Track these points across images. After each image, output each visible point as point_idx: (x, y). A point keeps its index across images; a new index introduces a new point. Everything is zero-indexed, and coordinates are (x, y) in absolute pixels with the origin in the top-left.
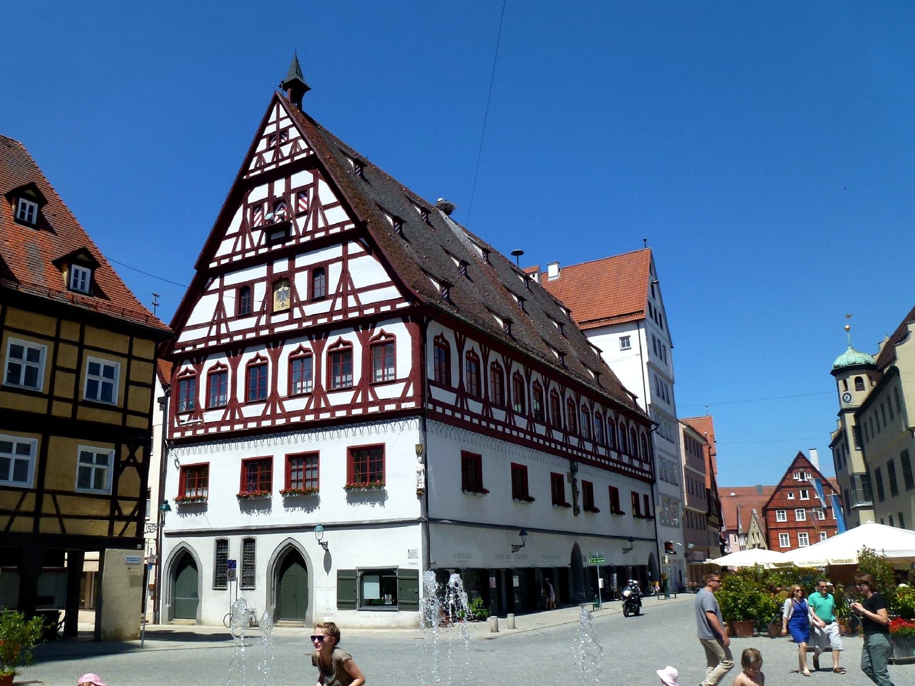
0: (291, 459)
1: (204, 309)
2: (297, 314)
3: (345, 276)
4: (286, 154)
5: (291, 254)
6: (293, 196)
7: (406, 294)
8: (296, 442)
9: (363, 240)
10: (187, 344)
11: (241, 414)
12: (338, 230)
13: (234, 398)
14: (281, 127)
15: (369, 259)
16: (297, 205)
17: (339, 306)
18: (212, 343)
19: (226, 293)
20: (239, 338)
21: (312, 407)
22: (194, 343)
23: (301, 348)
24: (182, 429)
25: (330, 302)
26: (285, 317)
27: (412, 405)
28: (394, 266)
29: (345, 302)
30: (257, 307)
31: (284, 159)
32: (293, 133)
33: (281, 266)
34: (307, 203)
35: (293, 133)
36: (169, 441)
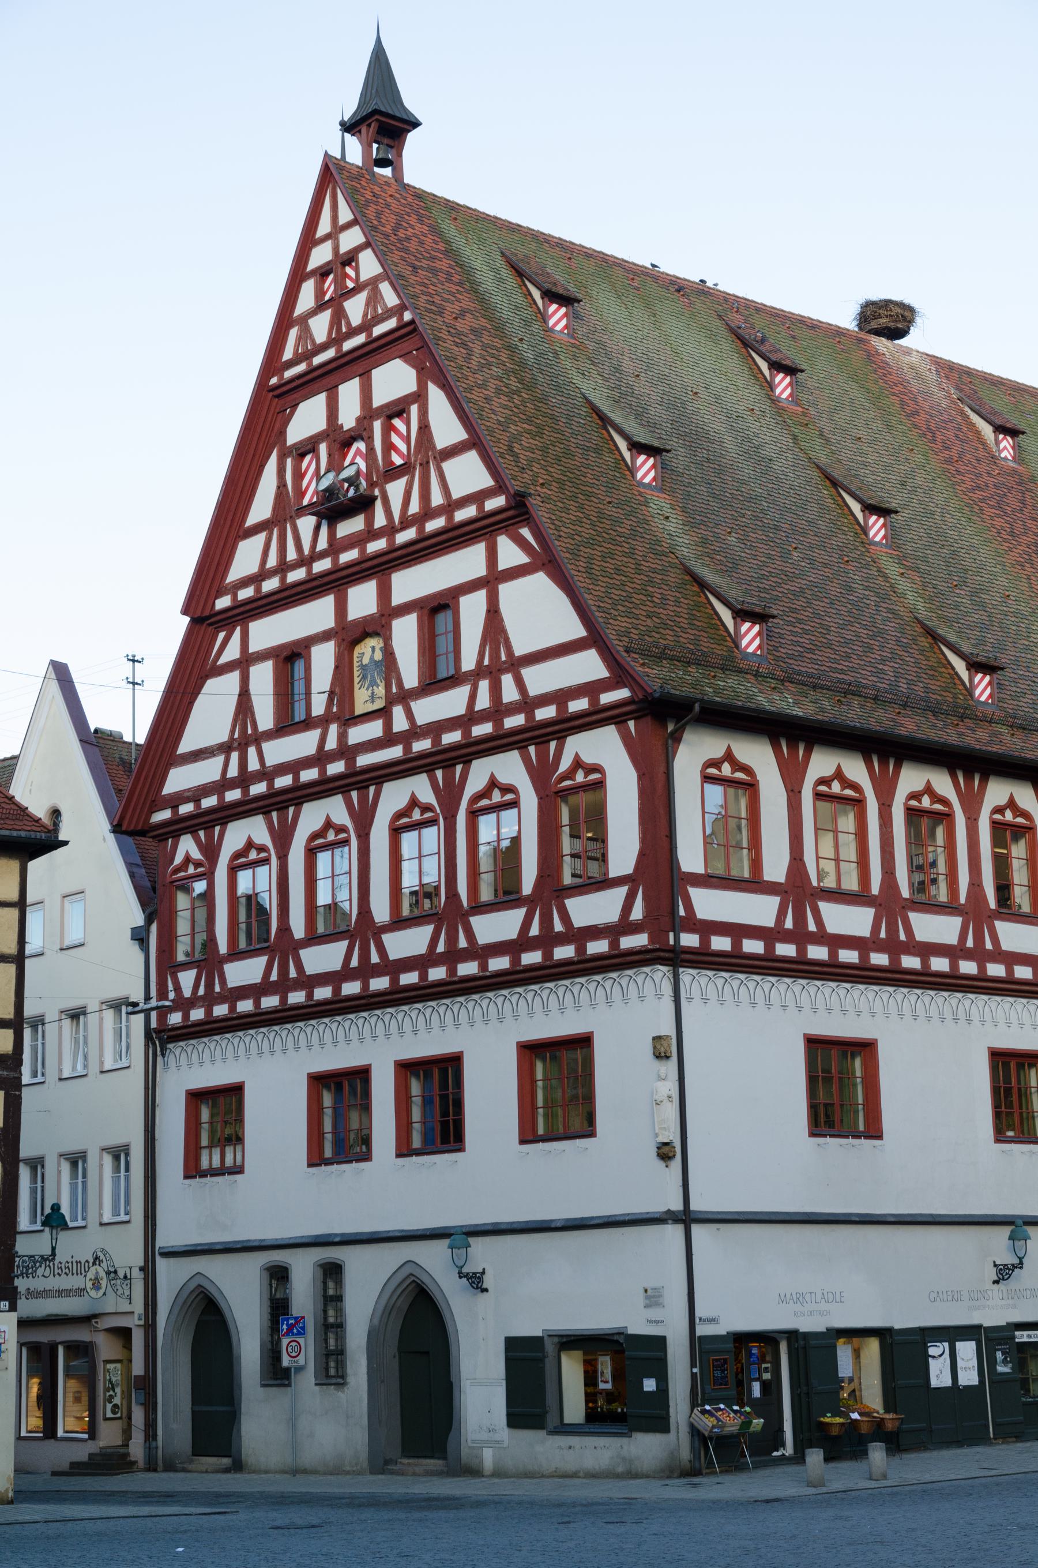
0: (406, 1069)
1: (211, 717)
2: (400, 723)
3: (494, 627)
4: (356, 320)
5: (380, 568)
6: (377, 425)
7: (619, 675)
8: (415, 1032)
9: (525, 532)
11: (300, 967)
13: (285, 928)
14: (343, 249)
15: (540, 580)
17: (483, 701)
18: (233, 795)
19: (255, 671)
20: (283, 782)
21: (441, 948)
22: (197, 794)
23: (414, 802)
24: (184, 1005)
26: (374, 729)
28: (590, 601)
29: (496, 690)
30: (318, 708)
31: (353, 332)
32: (369, 265)
33: (363, 600)
34: (407, 440)
35: (369, 265)
36: (158, 1031)
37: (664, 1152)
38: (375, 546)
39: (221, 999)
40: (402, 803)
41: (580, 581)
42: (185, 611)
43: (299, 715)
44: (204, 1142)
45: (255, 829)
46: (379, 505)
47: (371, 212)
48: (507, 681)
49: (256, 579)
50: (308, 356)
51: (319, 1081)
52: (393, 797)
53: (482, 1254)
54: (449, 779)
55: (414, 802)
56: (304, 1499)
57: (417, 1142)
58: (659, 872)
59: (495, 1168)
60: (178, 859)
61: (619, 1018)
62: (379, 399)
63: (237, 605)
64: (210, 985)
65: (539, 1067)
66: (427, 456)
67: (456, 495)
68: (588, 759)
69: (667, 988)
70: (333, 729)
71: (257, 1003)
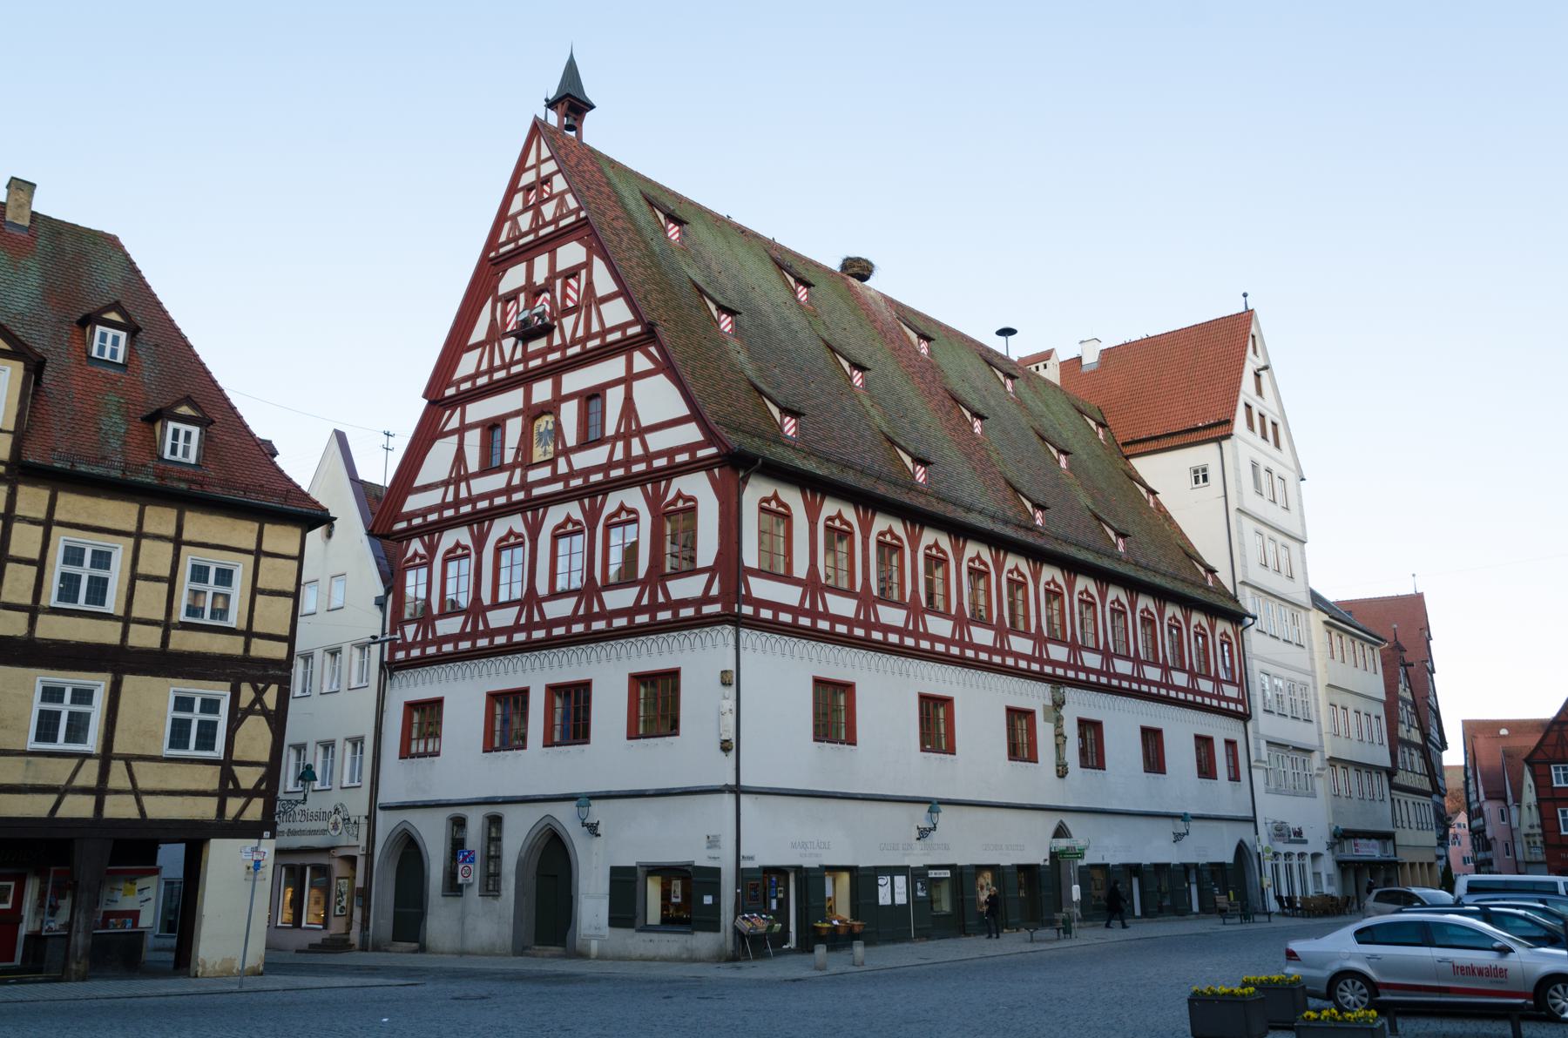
0: (553, 690)
2: (562, 467)
6: (559, 283)
7: (711, 437)
8: (561, 666)
9: (653, 349)
10: (414, 514)
12: (617, 336)
15: (661, 379)
16: (565, 296)
17: (619, 455)
18: (449, 513)
21: (581, 612)
22: (424, 513)
23: (569, 519)
24: (407, 647)
25: (607, 448)
26: (545, 472)
27: (716, 608)
29: (628, 448)
30: (509, 457)
32: (559, 184)
33: (542, 391)
34: (578, 292)
35: (559, 184)
37: (725, 747)
38: (551, 357)
39: (432, 643)
40: (561, 519)
41: (688, 379)
42: (425, 396)
43: (496, 463)
44: (414, 735)
45: (463, 535)
46: (557, 332)
47: (562, 152)
48: (636, 442)
49: (472, 377)
50: (515, 239)
51: (494, 697)
52: (555, 516)
53: (598, 811)
54: (593, 504)
55: (569, 519)
56: (468, 974)
57: (557, 738)
58: (729, 564)
59: (611, 753)
60: (410, 554)
61: (698, 659)
62: (560, 267)
63: (459, 393)
64: (425, 634)
65: (642, 691)
66: (591, 299)
67: (608, 325)
68: (686, 492)
69: (732, 641)
70: (518, 472)
71: (456, 646)
